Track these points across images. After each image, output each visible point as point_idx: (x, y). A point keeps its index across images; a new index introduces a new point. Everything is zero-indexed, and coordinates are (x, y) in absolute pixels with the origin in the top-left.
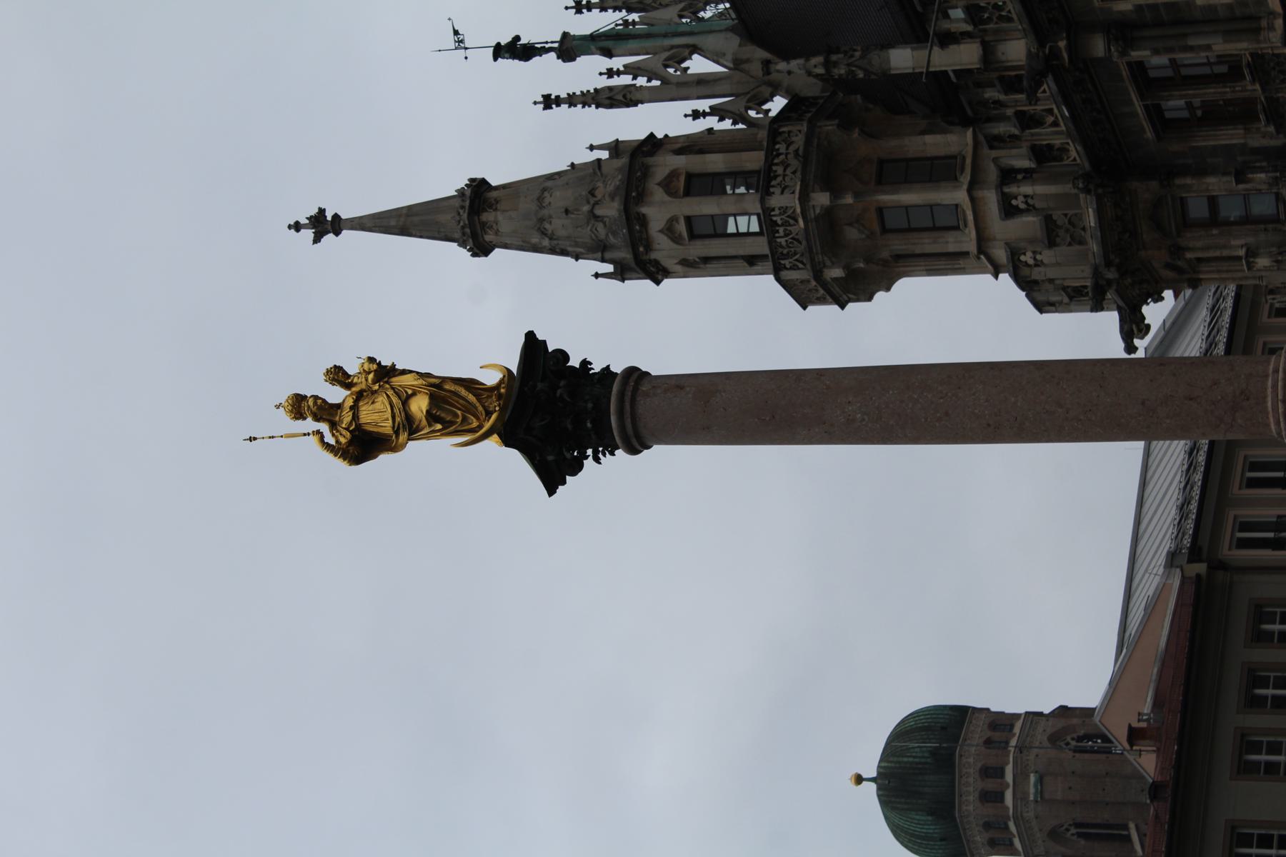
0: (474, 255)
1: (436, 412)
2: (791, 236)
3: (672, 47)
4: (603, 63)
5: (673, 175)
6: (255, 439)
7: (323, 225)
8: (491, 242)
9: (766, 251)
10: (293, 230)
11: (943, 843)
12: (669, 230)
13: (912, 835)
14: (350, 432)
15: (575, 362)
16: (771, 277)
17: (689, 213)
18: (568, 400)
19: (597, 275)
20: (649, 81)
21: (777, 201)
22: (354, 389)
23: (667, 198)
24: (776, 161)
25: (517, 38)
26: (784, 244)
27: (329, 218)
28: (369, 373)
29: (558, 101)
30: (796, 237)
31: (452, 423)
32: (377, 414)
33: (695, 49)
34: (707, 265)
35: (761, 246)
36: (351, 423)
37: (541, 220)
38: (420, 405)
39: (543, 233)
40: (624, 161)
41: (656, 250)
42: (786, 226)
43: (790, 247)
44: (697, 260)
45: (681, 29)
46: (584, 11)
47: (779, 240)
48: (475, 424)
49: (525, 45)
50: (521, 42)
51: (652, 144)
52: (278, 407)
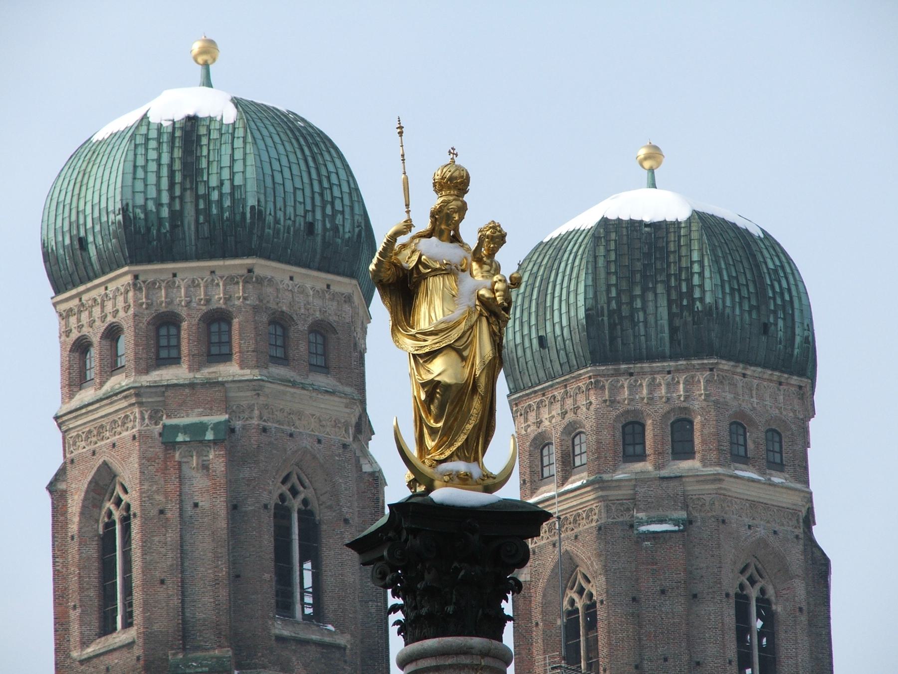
6: (401, 133)
11: (535, 342)
13: (545, 281)
18: (460, 577)
28: (493, 291)
31: (429, 411)
36: (426, 266)
48: (430, 443)
52: (453, 152)
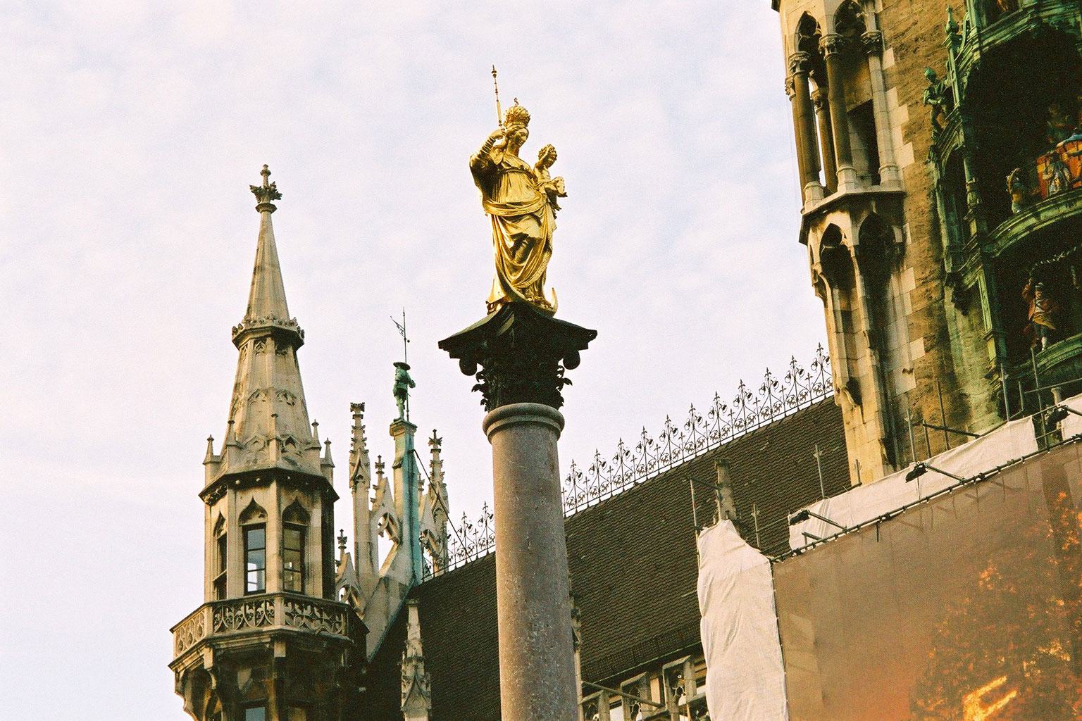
0: (235, 331)
1: (525, 243)
2: (245, 619)
3: (401, 524)
4: (389, 461)
5: (306, 517)
6: (495, 76)
7: (267, 196)
8: (247, 345)
9: (228, 598)
10: (263, 168)
12: (253, 508)
14: (500, 164)
15: (568, 374)
16: (203, 603)
17: (268, 527)
19: (211, 440)
20: (373, 501)
21: (279, 608)
22: (537, 173)
23: (283, 508)
24: (315, 609)
25: (413, 385)
26: (239, 613)
27: (272, 202)
29: (358, 417)
30: (245, 625)
31: (513, 257)
32: (515, 190)
33: (399, 541)
34: (216, 542)
35: (233, 592)
36: (509, 166)
37: (266, 392)
38: (529, 228)
39: (256, 394)
40: (319, 473)
41: (235, 493)
42: (256, 616)
43: (235, 619)
44: (222, 533)
45: (415, 533)
46: (432, 447)
47: (242, 608)
49: (406, 391)
50: (409, 387)
51: (330, 498)
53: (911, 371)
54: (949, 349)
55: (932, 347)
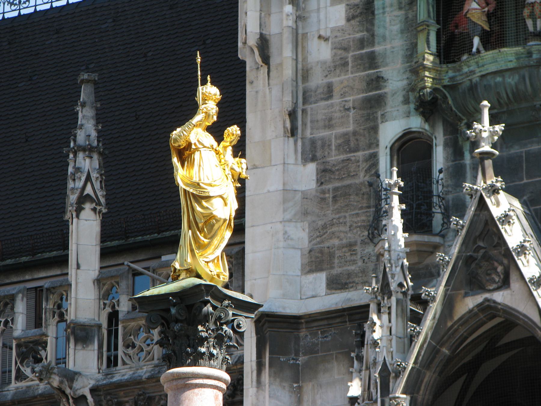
53: (326, 40)
54: (373, 24)
55: (354, 17)
